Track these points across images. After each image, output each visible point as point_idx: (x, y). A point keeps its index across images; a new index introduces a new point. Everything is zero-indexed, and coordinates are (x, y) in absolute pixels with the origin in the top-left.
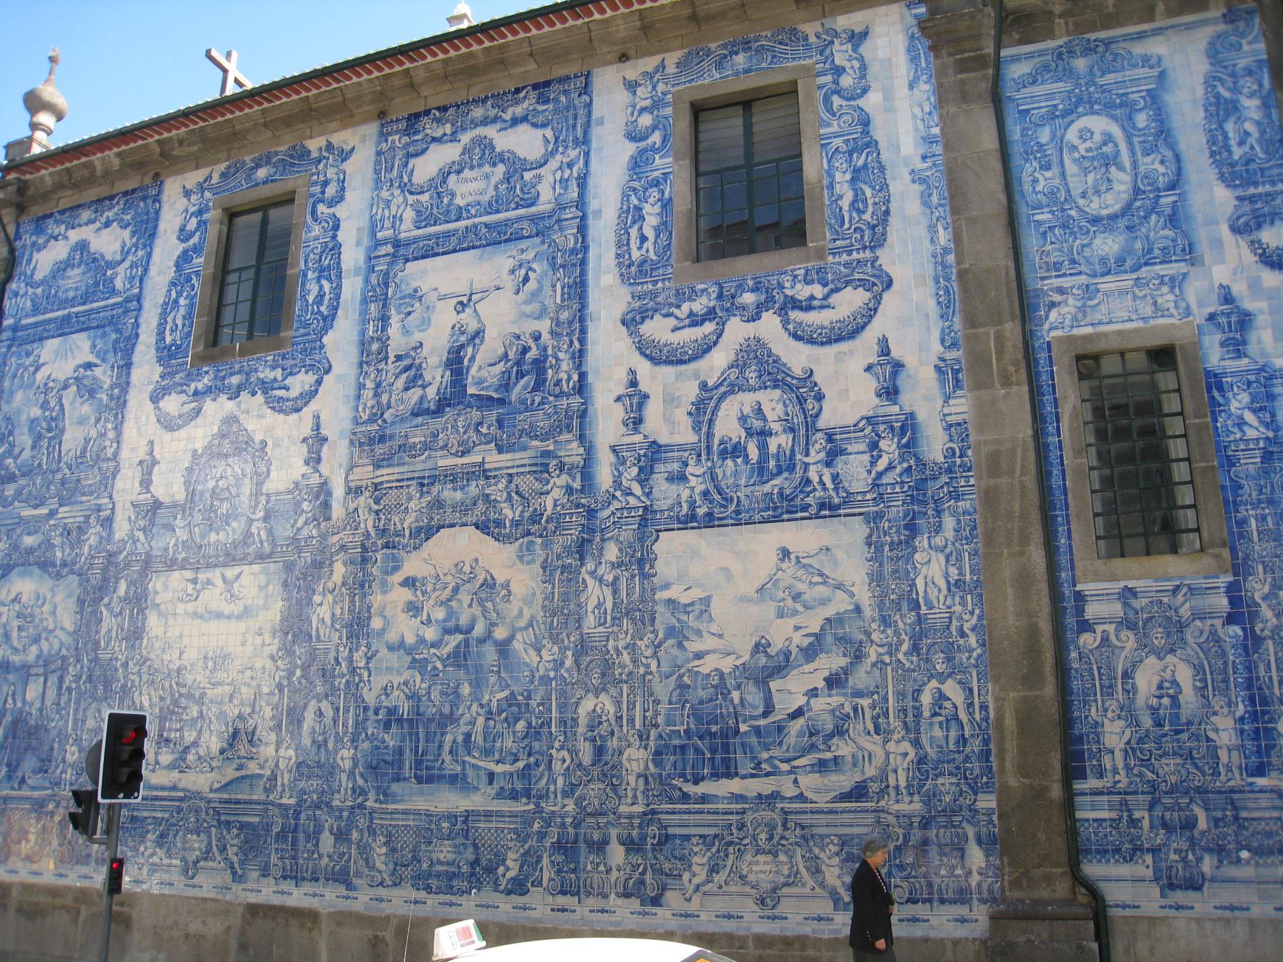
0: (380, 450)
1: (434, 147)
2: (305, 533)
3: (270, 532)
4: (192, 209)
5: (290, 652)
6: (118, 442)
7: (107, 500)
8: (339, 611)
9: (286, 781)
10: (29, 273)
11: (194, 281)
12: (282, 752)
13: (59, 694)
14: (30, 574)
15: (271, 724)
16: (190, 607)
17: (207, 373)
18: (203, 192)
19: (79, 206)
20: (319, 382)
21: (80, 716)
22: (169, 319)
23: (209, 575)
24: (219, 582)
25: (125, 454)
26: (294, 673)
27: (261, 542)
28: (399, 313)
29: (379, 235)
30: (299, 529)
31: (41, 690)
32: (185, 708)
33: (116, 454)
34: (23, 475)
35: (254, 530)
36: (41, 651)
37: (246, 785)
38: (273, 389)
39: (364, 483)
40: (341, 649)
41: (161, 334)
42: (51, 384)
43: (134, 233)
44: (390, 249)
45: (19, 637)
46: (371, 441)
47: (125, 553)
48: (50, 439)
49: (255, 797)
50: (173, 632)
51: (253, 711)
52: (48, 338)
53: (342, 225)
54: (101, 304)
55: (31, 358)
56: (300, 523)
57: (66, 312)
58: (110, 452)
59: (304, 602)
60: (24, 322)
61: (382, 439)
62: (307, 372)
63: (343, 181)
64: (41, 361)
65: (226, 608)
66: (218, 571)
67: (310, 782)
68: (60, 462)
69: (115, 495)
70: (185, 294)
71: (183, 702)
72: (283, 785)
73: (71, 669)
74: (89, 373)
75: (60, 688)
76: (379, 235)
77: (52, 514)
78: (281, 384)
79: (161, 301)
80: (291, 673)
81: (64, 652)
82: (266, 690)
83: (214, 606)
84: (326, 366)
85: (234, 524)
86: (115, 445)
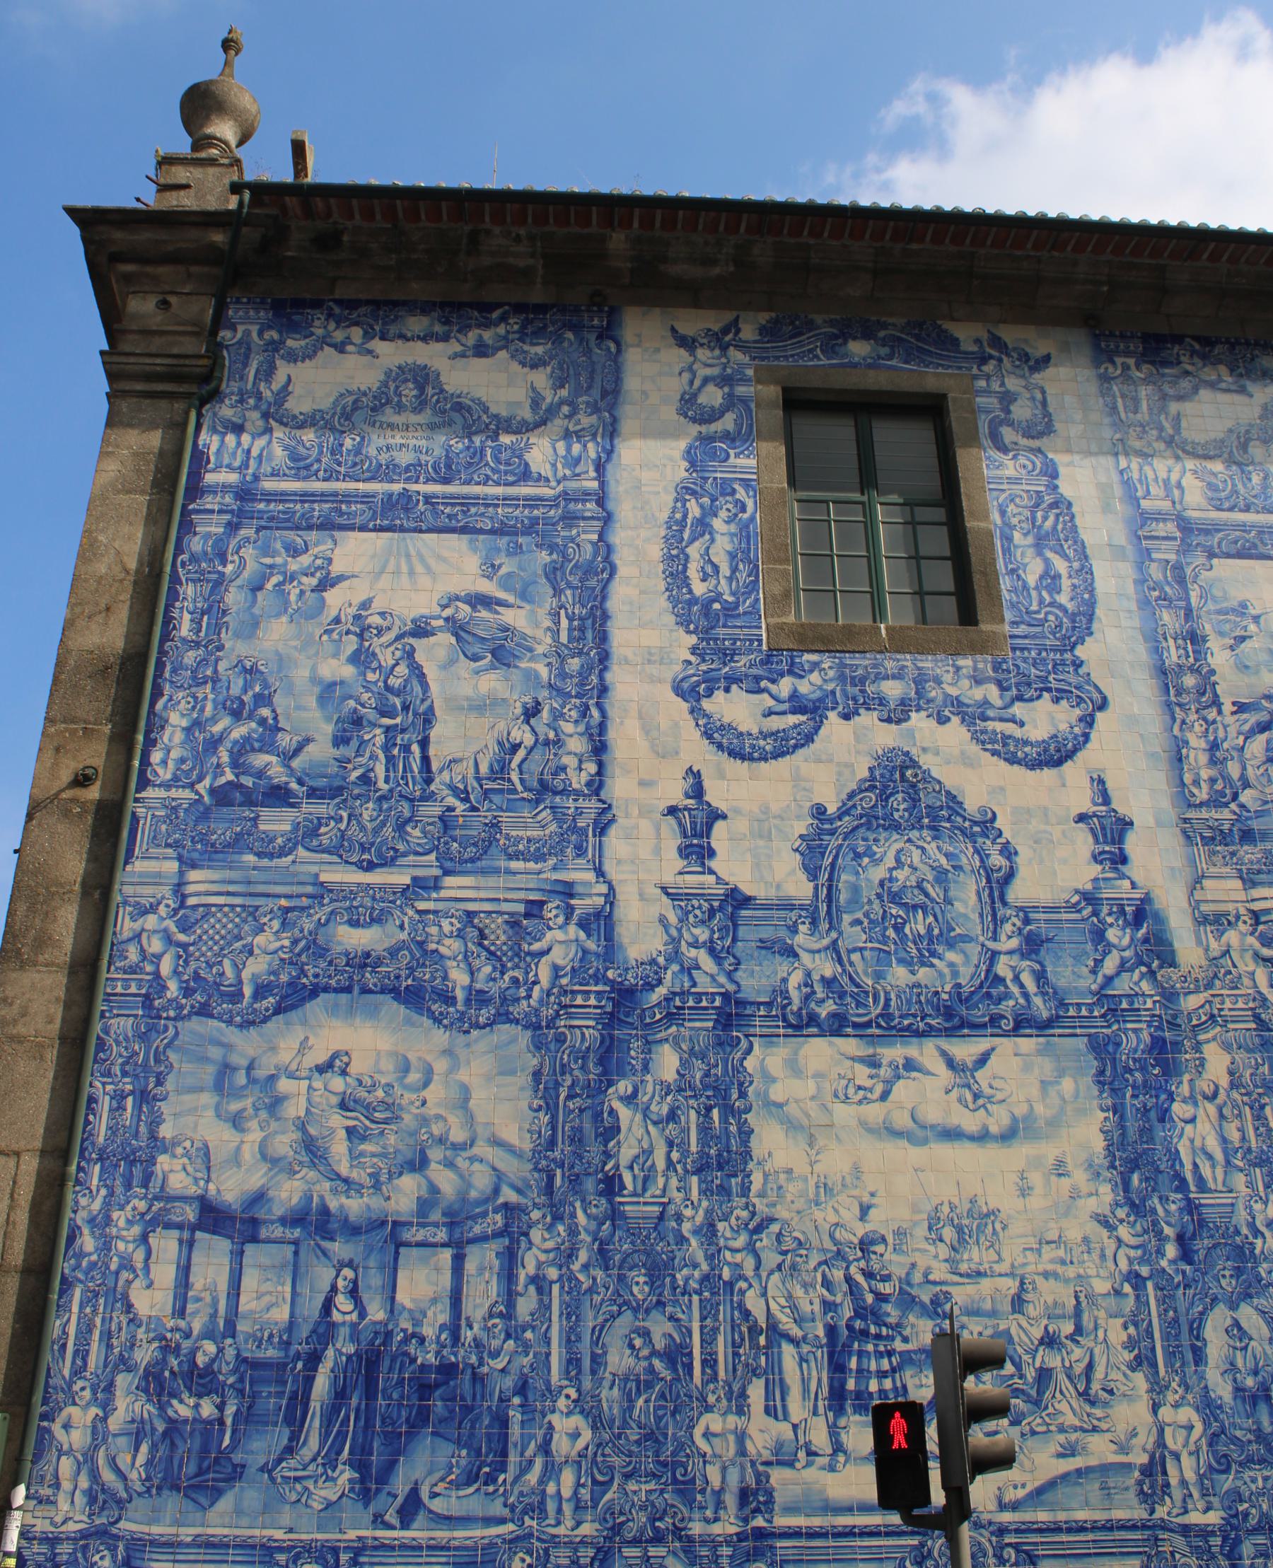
0: (1250, 854)
1: (1204, 394)
2: (1123, 985)
3: (1040, 976)
4: (703, 372)
5: (1137, 1208)
6: (601, 765)
7: (590, 876)
8: (1235, 1136)
9: (1190, 1475)
10: (267, 394)
11: (741, 494)
12: (1165, 1413)
13: (510, 1297)
14: (373, 1013)
15: (1128, 1356)
16: (874, 1112)
17: (815, 666)
18: (724, 348)
19: (395, 304)
20: (1089, 721)
21: (585, 1347)
22: (694, 551)
23: (911, 1050)
24: (940, 1067)
25: (620, 788)
26: (1160, 1252)
27: (1026, 995)
28: (1221, 634)
29: (1145, 504)
30: (1109, 980)
31: (446, 1279)
32: (898, 1327)
33: (596, 785)
34: (313, 793)
35: (1002, 969)
36: (434, 1189)
37: (1092, 1487)
38: (985, 719)
39: (1230, 907)
40: (1258, 1207)
41: (677, 576)
42: (375, 620)
43: (559, 383)
44: (1170, 528)
45: (354, 1156)
46: (1217, 837)
47: (661, 991)
48: (388, 729)
49: (1119, 1514)
50: (835, 1162)
51: (1079, 1330)
52: (351, 528)
53: (1061, 470)
54: (499, 490)
55: (305, 560)
56: (1110, 965)
57: (397, 488)
58: (578, 780)
59: (1153, 1114)
60: (269, 485)
61: (1248, 836)
62: (1056, 700)
63: (1044, 403)
64: (336, 569)
65: (969, 1122)
66: (930, 1045)
67: (1248, 1474)
68: (429, 781)
69: (608, 867)
70: (723, 514)
71: (892, 1312)
72: (1183, 1483)
73: (536, 1235)
74: (484, 614)
75: (508, 1275)
76: (1144, 503)
77: (421, 886)
78: (1003, 713)
79: (665, 515)
80: (1150, 1254)
81: (509, 1195)
82: (1101, 1286)
83: (932, 1115)
84: (1096, 695)
85: (951, 956)
86: (592, 768)
